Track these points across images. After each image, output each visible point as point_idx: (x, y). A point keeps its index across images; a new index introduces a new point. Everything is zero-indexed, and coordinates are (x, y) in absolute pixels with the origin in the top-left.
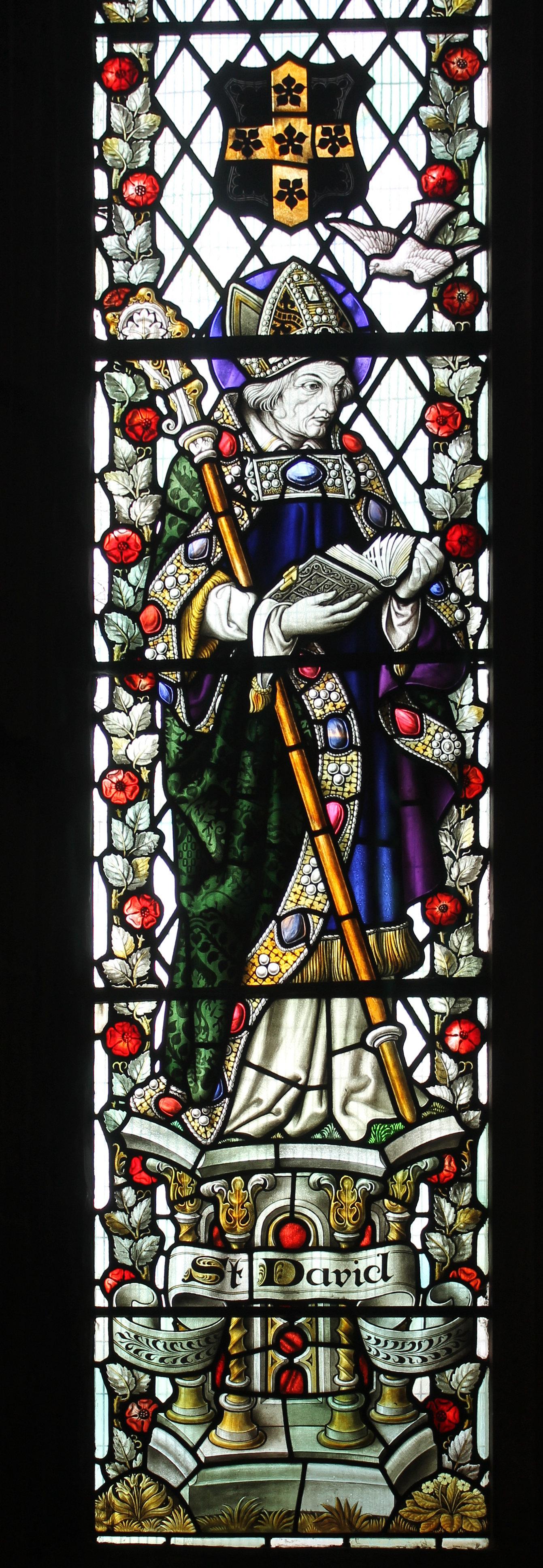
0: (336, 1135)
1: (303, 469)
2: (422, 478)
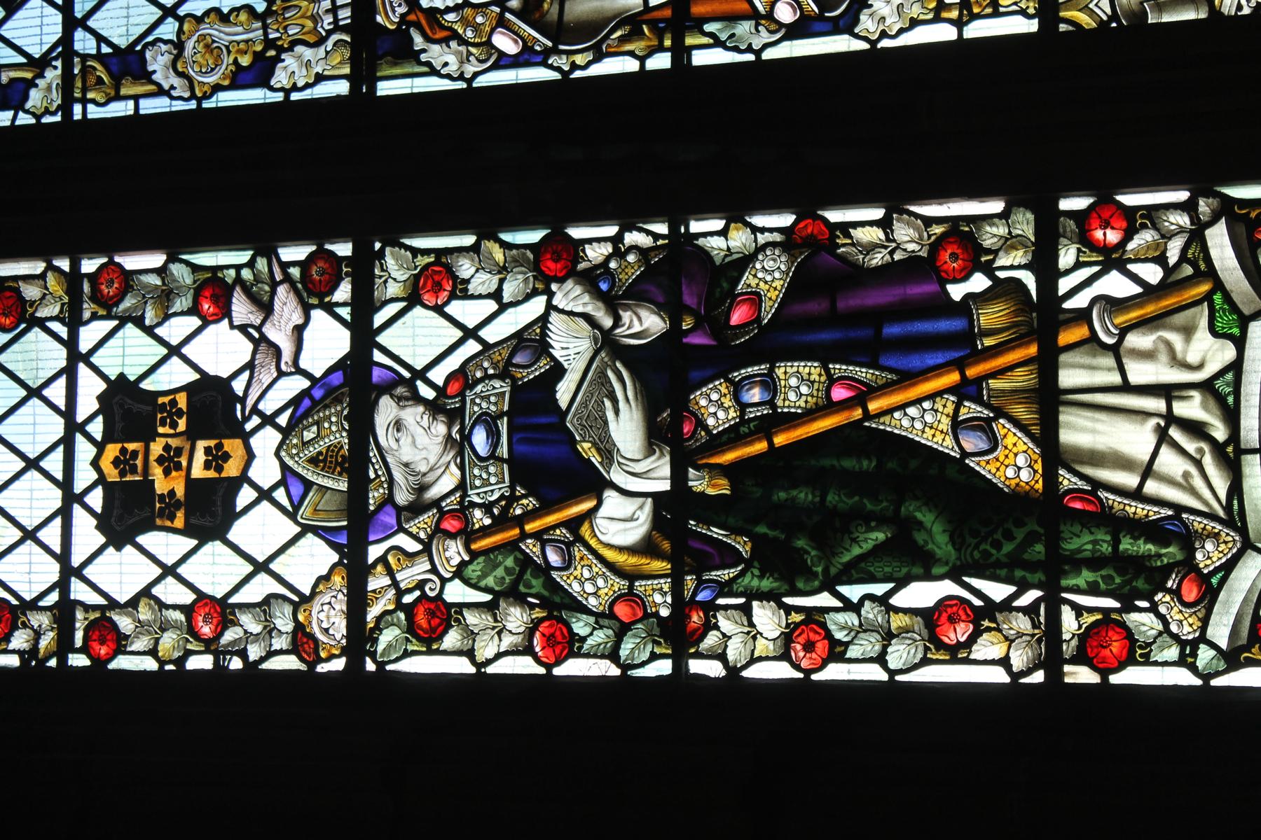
0: (1229, 376)
1: (480, 439)
2: (492, 306)
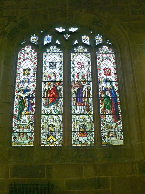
1: (26, 88)
